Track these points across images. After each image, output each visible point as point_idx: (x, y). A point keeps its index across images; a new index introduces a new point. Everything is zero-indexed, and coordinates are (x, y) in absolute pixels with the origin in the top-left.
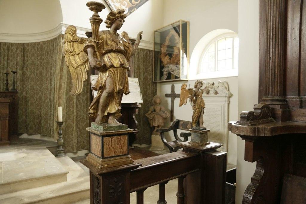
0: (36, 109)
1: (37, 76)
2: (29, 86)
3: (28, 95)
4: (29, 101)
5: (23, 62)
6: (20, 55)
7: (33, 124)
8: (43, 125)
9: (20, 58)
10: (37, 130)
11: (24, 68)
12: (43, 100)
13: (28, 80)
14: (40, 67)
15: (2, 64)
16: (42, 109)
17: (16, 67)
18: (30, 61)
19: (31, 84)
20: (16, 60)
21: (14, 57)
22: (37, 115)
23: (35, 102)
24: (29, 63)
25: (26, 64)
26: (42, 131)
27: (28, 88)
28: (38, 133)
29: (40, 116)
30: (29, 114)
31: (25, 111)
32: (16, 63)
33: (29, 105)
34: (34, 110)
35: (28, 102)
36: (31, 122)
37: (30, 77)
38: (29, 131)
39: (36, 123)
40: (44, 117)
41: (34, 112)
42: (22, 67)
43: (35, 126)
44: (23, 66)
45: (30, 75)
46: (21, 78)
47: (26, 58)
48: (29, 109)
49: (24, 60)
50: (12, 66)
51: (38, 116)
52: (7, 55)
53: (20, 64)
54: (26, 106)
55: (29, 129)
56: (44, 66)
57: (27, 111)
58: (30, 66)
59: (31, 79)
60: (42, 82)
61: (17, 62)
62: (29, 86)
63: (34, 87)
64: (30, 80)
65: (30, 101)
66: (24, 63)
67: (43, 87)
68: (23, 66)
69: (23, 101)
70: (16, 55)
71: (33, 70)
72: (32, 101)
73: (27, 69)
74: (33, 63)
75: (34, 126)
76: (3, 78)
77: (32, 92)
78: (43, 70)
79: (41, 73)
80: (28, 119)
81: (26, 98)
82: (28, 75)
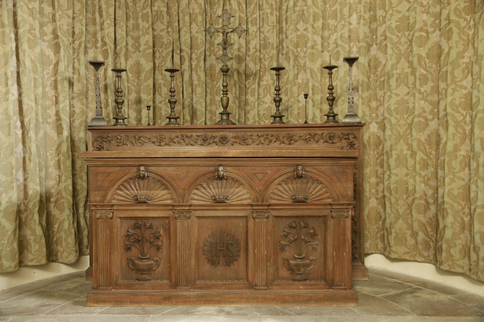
0: (418, 178)
1: (420, 64)
2: (392, 103)
3: (388, 132)
4: (391, 151)
5: (370, 27)
6: (361, 8)
7: (405, 226)
8: (448, 234)
9: (360, 17)
10: (420, 247)
11: (371, 46)
12: (450, 147)
13: (388, 83)
14: (434, 32)
15: (309, 45)
16: (447, 180)
17: (346, 46)
18: (394, 19)
19: (397, 95)
20: (347, 24)
21: (342, 18)
22: (420, 198)
23: (413, 155)
24: (389, 27)
25: (381, 30)
26: (444, 254)
27: (389, 109)
28: (423, 259)
29: (431, 201)
30: (391, 194)
31: (377, 184)
32: (346, 35)
33: (392, 162)
34: (411, 182)
35: (389, 156)
36: (401, 221)
37: (395, 72)
38: (393, 249)
39: (416, 225)
40: (452, 207)
41: (410, 188)
42: (367, 43)
43: (415, 235)
44: (369, 40)
45: (392, 65)
46: (366, 80)
47: (380, 13)
48: (393, 178)
49: (374, 19)
50: (337, 46)
51: (423, 202)
52: (321, 13)
53: (362, 36)
54: (382, 166)
55: (392, 242)
56: (452, 25)
57: (386, 183)
58: (394, 37)
59: (397, 79)
60: (442, 85)
61: (350, 31)
62: (392, 103)
63: (411, 106)
64: (393, 82)
65: (394, 152)
66: (374, 32)
67: (449, 99)
68: (369, 40)
69: (371, 153)
70: (346, 11)
71: (403, 48)
72: (402, 150)
73: (384, 49)
74: (407, 25)
75: (409, 232)
76: (313, 85)
77: (402, 122)
78: (449, 39)
79: (438, 53)
80: (388, 210)
81: (379, 142)
82: (389, 67)
